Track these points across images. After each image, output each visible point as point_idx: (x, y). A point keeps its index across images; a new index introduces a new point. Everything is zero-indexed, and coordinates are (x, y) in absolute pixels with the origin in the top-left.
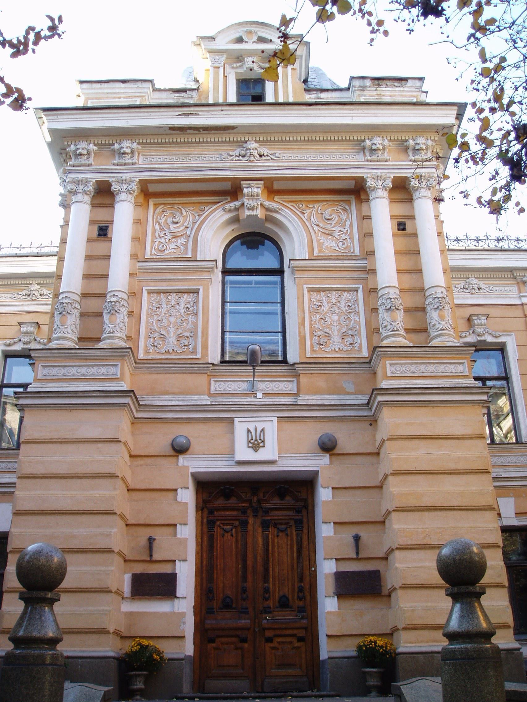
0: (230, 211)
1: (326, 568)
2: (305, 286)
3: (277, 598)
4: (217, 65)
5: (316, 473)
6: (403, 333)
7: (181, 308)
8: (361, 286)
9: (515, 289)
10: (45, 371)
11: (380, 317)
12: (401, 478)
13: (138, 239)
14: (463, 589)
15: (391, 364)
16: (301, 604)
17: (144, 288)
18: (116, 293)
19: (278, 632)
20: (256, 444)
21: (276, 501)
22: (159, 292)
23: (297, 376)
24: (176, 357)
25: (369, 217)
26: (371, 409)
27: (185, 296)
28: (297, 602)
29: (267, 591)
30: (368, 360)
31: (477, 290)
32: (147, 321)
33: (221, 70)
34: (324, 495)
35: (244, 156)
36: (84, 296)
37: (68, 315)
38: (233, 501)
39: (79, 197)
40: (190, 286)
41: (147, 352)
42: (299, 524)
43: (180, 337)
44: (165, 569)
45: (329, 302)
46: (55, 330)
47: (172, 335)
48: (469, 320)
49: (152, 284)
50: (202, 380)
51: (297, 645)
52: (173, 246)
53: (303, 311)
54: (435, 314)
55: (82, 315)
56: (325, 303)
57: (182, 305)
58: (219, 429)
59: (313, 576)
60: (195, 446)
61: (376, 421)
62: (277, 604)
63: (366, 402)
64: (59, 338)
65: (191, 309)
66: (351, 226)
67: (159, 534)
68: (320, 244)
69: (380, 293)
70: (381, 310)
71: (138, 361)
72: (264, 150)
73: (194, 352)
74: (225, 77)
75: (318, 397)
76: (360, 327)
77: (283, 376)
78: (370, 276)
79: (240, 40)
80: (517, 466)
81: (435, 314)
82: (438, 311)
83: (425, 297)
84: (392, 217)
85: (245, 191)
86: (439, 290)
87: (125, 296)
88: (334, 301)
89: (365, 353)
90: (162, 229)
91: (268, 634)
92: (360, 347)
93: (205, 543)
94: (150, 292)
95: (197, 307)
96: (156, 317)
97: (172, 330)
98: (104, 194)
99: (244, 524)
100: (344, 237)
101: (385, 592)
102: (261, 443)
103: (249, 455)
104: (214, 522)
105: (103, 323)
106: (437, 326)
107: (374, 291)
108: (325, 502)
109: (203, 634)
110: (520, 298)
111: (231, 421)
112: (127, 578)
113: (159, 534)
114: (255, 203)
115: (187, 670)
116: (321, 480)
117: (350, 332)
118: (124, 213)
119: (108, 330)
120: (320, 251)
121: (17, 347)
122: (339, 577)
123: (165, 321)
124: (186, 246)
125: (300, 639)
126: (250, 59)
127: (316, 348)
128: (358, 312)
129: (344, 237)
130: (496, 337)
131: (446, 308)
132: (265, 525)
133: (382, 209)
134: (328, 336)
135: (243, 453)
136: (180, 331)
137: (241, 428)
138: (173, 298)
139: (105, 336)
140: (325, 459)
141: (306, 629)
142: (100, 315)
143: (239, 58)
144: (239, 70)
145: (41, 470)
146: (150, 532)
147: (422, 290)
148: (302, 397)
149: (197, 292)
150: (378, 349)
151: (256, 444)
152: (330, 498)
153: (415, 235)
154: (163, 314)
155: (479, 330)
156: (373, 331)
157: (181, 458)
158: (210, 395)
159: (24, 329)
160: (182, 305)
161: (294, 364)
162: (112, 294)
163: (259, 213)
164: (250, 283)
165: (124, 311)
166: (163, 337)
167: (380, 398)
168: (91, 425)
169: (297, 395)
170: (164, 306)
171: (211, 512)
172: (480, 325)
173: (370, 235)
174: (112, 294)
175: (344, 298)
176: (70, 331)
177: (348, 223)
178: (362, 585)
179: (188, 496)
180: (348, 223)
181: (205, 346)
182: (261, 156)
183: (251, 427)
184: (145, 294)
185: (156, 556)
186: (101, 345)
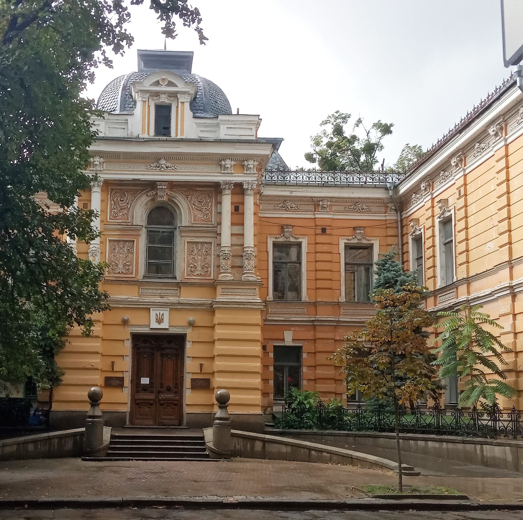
0: (150, 196)
4: (144, 100)
16: (176, 390)
19: (166, 402)
20: (159, 321)
21: (166, 345)
22: (114, 241)
25: (221, 203)
29: (162, 384)
31: (290, 208)
33: (147, 102)
35: (158, 167)
38: (147, 345)
42: (177, 355)
43: (125, 265)
44: (120, 375)
51: (173, 406)
52: (121, 214)
54: (246, 262)
56: (195, 250)
58: (144, 314)
66: (212, 205)
68: (195, 216)
72: (169, 164)
73: (131, 273)
74: (149, 106)
79: (157, 83)
81: (246, 262)
84: (232, 203)
85: (158, 187)
86: (250, 249)
87: (98, 246)
90: (115, 204)
91: (162, 402)
93: (136, 363)
94: (110, 241)
97: (121, 261)
99: (153, 354)
100: (207, 212)
101: (211, 387)
107: (219, 245)
109: (135, 402)
110: (314, 214)
111: (149, 309)
114: (163, 197)
116: (188, 338)
117: (206, 266)
120: (194, 221)
122: (193, 380)
124: (127, 215)
125: (176, 405)
126: (163, 96)
129: (207, 212)
130: (296, 238)
132: (162, 355)
133: (227, 201)
134: (195, 267)
135: (154, 325)
137: (153, 313)
141: (177, 400)
143: (157, 94)
144: (156, 101)
151: (159, 321)
153: (243, 214)
163: (165, 199)
171: (138, 349)
172: (288, 231)
173: (220, 213)
177: (210, 204)
178: (203, 384)
180: (210, 204)
182: (167, 167)
183: (158, 313)
184: (108, 241)
185: (115, 370)
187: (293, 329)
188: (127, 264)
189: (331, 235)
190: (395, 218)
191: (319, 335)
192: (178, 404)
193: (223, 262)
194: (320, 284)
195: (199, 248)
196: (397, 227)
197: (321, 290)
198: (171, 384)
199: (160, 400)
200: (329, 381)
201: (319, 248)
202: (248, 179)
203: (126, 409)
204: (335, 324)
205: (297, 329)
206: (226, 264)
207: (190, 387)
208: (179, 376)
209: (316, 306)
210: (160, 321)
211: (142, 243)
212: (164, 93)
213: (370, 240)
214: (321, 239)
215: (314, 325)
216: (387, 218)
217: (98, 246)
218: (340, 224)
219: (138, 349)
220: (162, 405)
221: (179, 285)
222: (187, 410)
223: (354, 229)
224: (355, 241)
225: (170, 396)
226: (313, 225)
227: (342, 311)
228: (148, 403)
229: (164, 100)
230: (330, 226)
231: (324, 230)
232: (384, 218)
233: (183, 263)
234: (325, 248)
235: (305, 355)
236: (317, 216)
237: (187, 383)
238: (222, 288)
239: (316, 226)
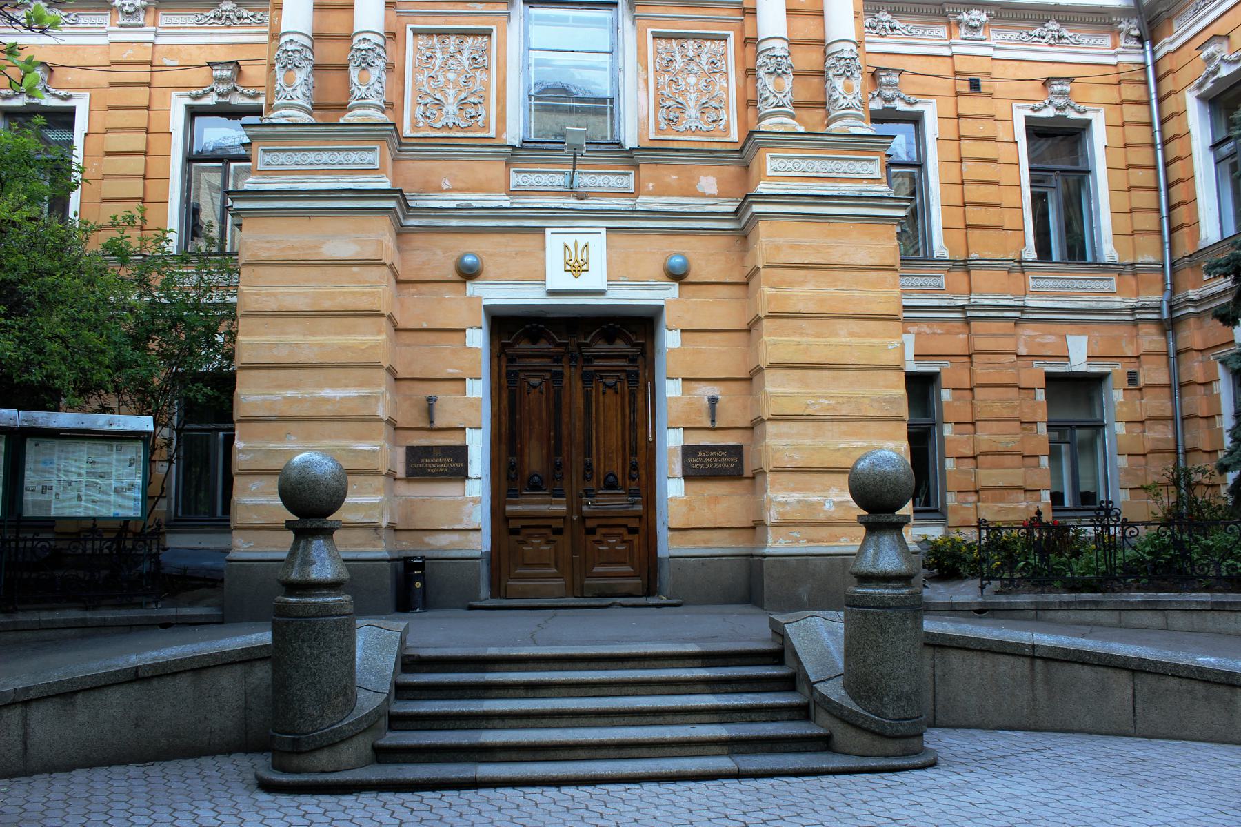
1: (672, 440)
2: (649, 30)
3: (602, 477)
5: (659, 309)
6: (790, 109)
7: (465, 58)
8: (732, 33)
9: (944, 32)
10: (268, 158)
11: (759, 84)
12: (779, 322)
14: (884, 518)
15: (772, 157)
16: (634, 485)
17: (409, 27)
18: (368, 36)
20: (576, 267)
21: (602, 347)
22: (430, 33)
23: (636, 167)
24: (458, 135)
26: (739, 220)
27: (471, 39)
28: (628, 482)
29: (588, 467)
30: (738, 147)
32: (414, 77)
34: (670, 340)
36: (317, 37)
37: (296, 70)
40: (478, 24)
41: (415, 127)
42: (632, 377)
43: (463, 104)
45: (684, 55)
46: (278, 93)
47: (451, 100)
48: (873, 75)
49: (420, 19)
50: (496, 169)
51: (627, 537)
53: (646, 68)
54: (839, 83)
55: (317, 68)
57: (466, 54)
59: (651, 449)
60: (490, 268)
61: (746, 237)
62: (602, 485)
63: (733, 209)
64: (284, 107)
65: (480, 60)
67: (442, 393)
69: (762, 47)
70: (761, 73)
71: (403, 141)
73: (484, 128)
75: (663, 199)
76: (728, 96)
77: (615, 167)
78: (748, 20)
80: (924, 291)
81: (839, 83)
82: (843, 79)
83: (826, 57)
87: (380, 41)
88: (691, 54)
89: (734, 136)
91: (590, 524)
92: (727, 127)
93: (505, 402)
95: (489, 57)
96: (426, 72)
97: (451, 92)
99: (558, 376)
103: (569, 283)
104: (517, 374)
105: (348, 82)
106: (841, 101)
107: (750, 42)
108: (672, 350)
110: (950, 46)
111: (542, 230)
112: (401, 454)
113: (442, 393)
115: (484, 571)
116: (667, 318)
117: (714, 103)
119: (357, 93)
121: (211, 100)
122: (688, 451)
123: (441, 78)
125: (633, 531)
127: (663, 126)
128: (726, 73)
131: (856, 75)
132: (587, 378)
134: (681, 107)
135: (558, 278)
136: (463, 95)
137: (556, 243)
138: (452, 41)
139: (353, 102)
140: (674, 290)
141: (640, 517)
142: (345, 68)
145: (273, 305)
147: (822, 43)
148: (641, 199)
149: (487, 33)
150: (756, 135)
151: (576, 267)
152: (678, 345)
154: (437, 68)
155: (889, 93)
156: (749, 103)
157: (469, 284)
158: (511, 193)
159: (217, 73)
160: (466, 54)
161: (631, 149)
162: (361, 37)
164: (566, 19)
165: (380, 63)
166: (439, 103)
167: (756, 208)
168: (342, 240)
169: (635, 195)
170: (439, 55)
171: (511, 360)
174: (361, 37)
175: (706, 49)
176: (300, 95)
178: (716, 465)
179: (478, 339)
181: (502, 119)
184: (409, 34)
185: (438, 423)
186: (348, 118)
187: (914, 328)
188: (473, 99)
189: (990, 95)
190: (1140, 59)
191: (981, 344)
192: (643, 527)
193: (767, 82)
194: (975, 216)
195: (691, 54)
196: (1146, 82)
197: (977, 232)
198: (616, 466)
199: (583, 519)
200: (1008, 460)
201: (967, 127)
203: (481, 543)
204: (1018, 314)
205: (924, 328)
206: (777, 90)
207: (680, 475)
208: (642, 443)
209: (968, 272)
210: (578, 266)
213: (1084, 112)
214: (969, 105)
215: (966, 315)
216: (1122, 58)
217: (380, 41)
218: (1011, 71)
219: (511, 360)
220: (591, 532)
221: (632, 158)
222: (668, 546)
223: (1047, 82)
224: (1049, 112)
225: (614, 502)
226: (950, 73)
227: (1032, 283)
228: (550, 528)
230: (988, 75)
231: (975, 85)
232: (1113, 61)
233: (642, 94)
234: (982, 128)
235: (946, 395)
236: (956, 49)
238: (772, 157)
239: (955, 73)
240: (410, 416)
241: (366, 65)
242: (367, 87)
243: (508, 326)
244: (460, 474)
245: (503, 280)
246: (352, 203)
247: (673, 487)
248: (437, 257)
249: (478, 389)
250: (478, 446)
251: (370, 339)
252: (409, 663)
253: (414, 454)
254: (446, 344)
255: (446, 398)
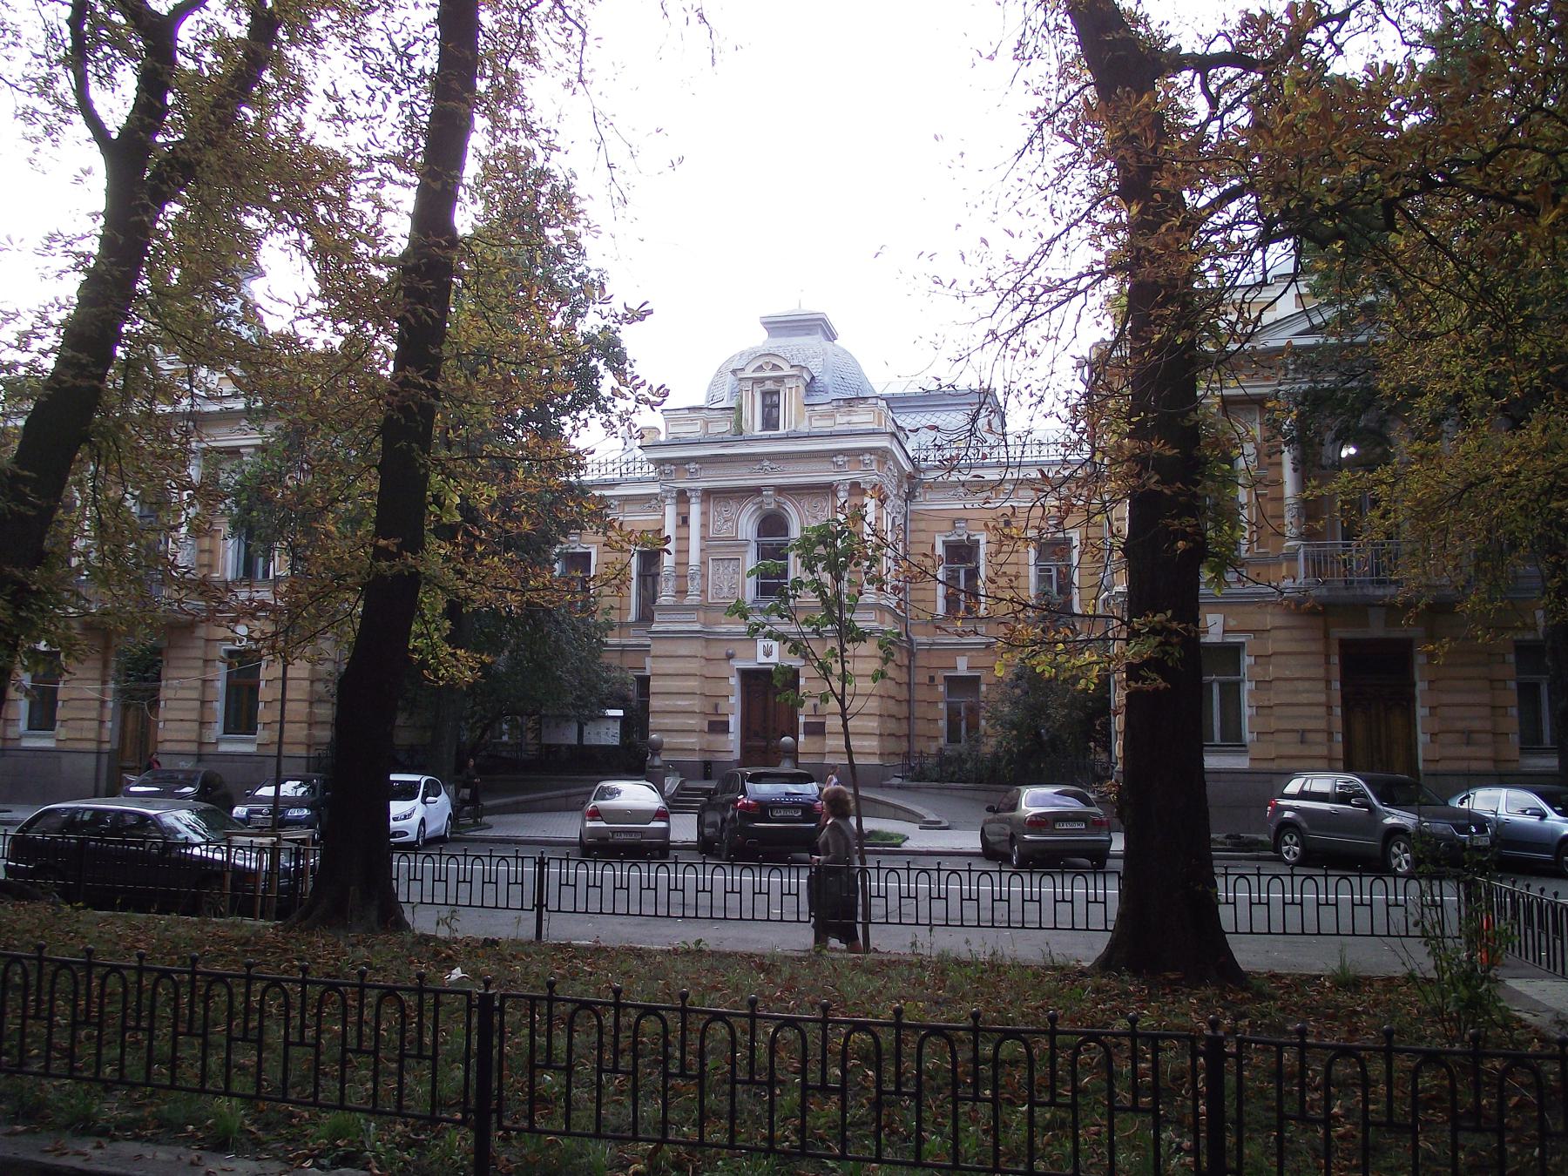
1: (802, 719)
13: (704, 526)
20: (768, 654)
39: (668, 501)
60: (738, 654)
67: (722, 702)
98: (682, 497)
102: (768, 654)
109: (744, 748)
118: (695, 510)
135: (762, 659)
137: (761, 644)
143: (762, 380)
146: (714, 700)
151: (768, 654)
168: (684, 648)
179: (734, 681)
202: (868, 475)
211: (750, 560)
212: (769, 378)
229: (769, 386)
237: (801, 729)
240: (709, 709)
241: (693, 579)
242: (693, 587)
243: (745, 675)
244: (727, 731)
245: (742, 659)
246: (690, 636)
247: (801, 738)
248: (719, 651)
249: (735, 700)
250: (734, 722)
251: (692, 684)
252: (681, 787)
253: (711, 723)
254: (723, 683)
255: (722, 702)
